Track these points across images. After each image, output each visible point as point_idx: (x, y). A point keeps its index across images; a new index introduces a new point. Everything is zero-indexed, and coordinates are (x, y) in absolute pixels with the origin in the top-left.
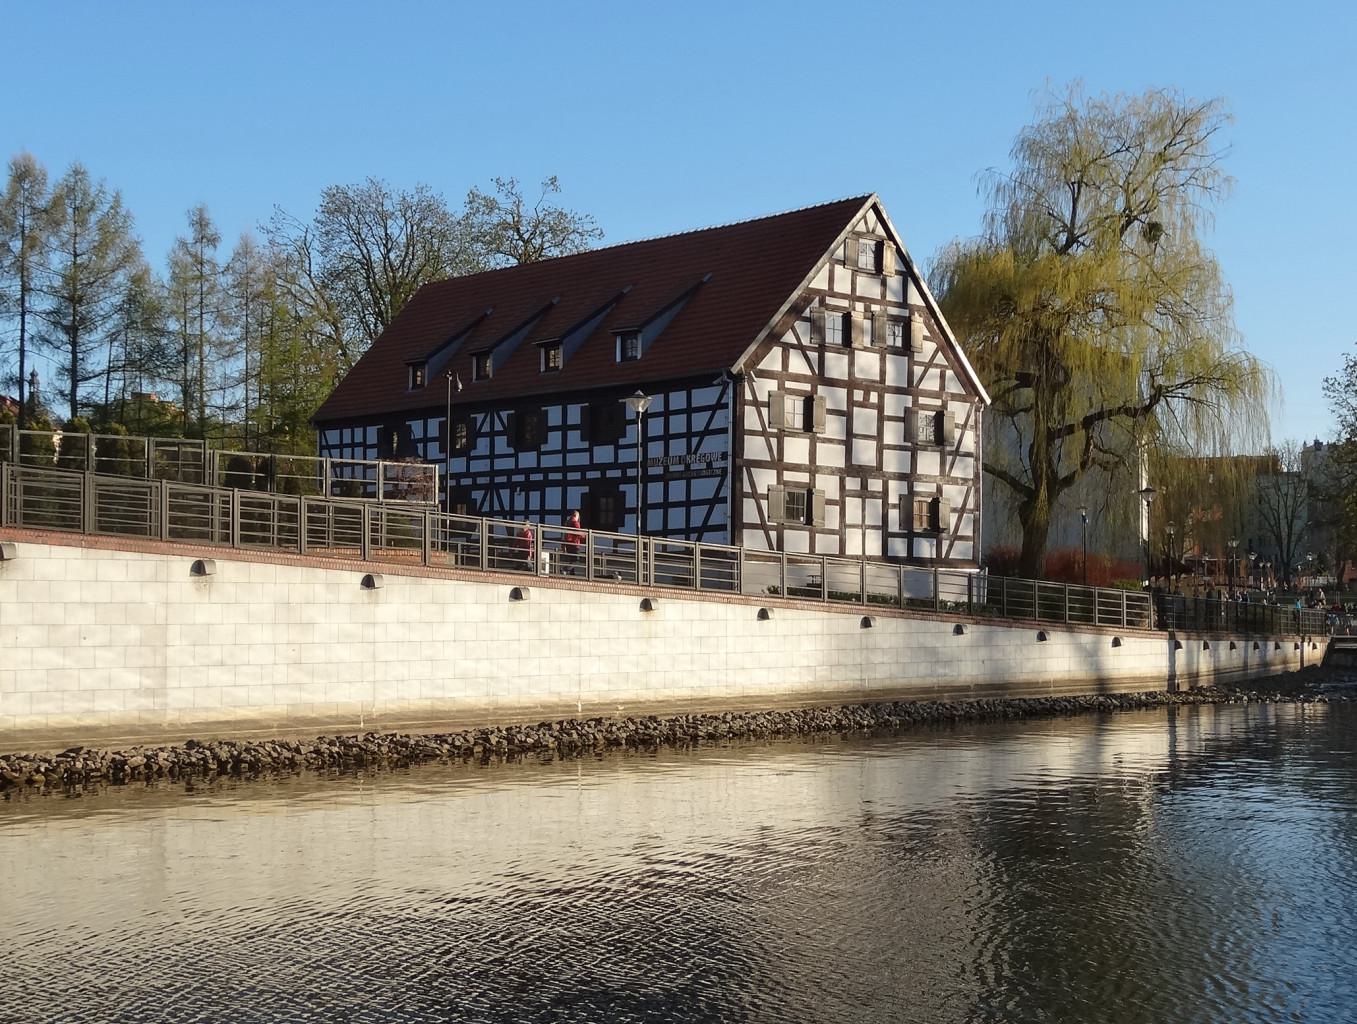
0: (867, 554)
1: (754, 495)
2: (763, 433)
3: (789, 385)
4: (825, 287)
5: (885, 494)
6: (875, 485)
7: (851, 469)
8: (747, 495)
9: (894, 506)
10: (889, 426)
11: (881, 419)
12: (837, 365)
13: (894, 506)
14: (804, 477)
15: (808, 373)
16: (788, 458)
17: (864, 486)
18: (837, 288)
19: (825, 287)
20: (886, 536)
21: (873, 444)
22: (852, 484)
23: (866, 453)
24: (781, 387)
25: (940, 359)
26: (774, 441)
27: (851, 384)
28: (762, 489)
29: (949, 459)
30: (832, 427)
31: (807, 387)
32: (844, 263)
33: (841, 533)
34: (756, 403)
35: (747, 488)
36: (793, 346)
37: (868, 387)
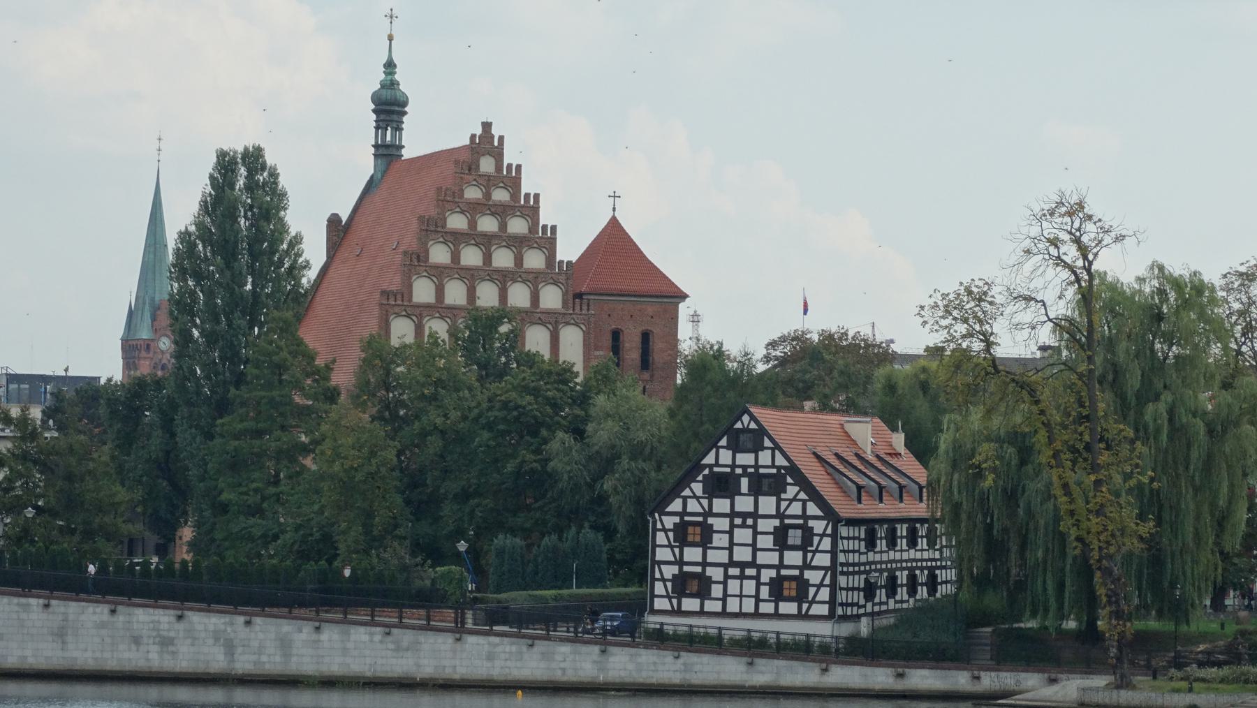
0: (743, 611)
1: (663, 580)
2: (670, 546)
3: (686, 518)
4: (713, 462)
5: (757, 578)
6: (750, 572)
7: (732, 563)
8: (658, 580)
9: (765, 584)
10: (759, 536)
11: (756, 533)
12: (721, 505)
13: (765, 584)
14: (698, 569)
15: (702, 511)
16: (686, 559)
17: (742, 572)
18: (720, 463)
19: (713, 462)
20: (758, 600)
21: (750, 549)
22: (734, 571)
23: (743, 554)
24: (682, 519)
25: (802, 496)
26: (677, 551)
27: (733, 514)
28: (668, 575)
29: (810, 555)
30: (720, 540)
31: (700, 519)
32: (727, 448)
33: (724, 600)
34: (665, 530)
35: (657, 575)
36: (690, 497)
37: (744, 515)
